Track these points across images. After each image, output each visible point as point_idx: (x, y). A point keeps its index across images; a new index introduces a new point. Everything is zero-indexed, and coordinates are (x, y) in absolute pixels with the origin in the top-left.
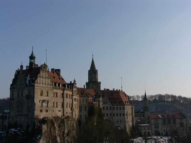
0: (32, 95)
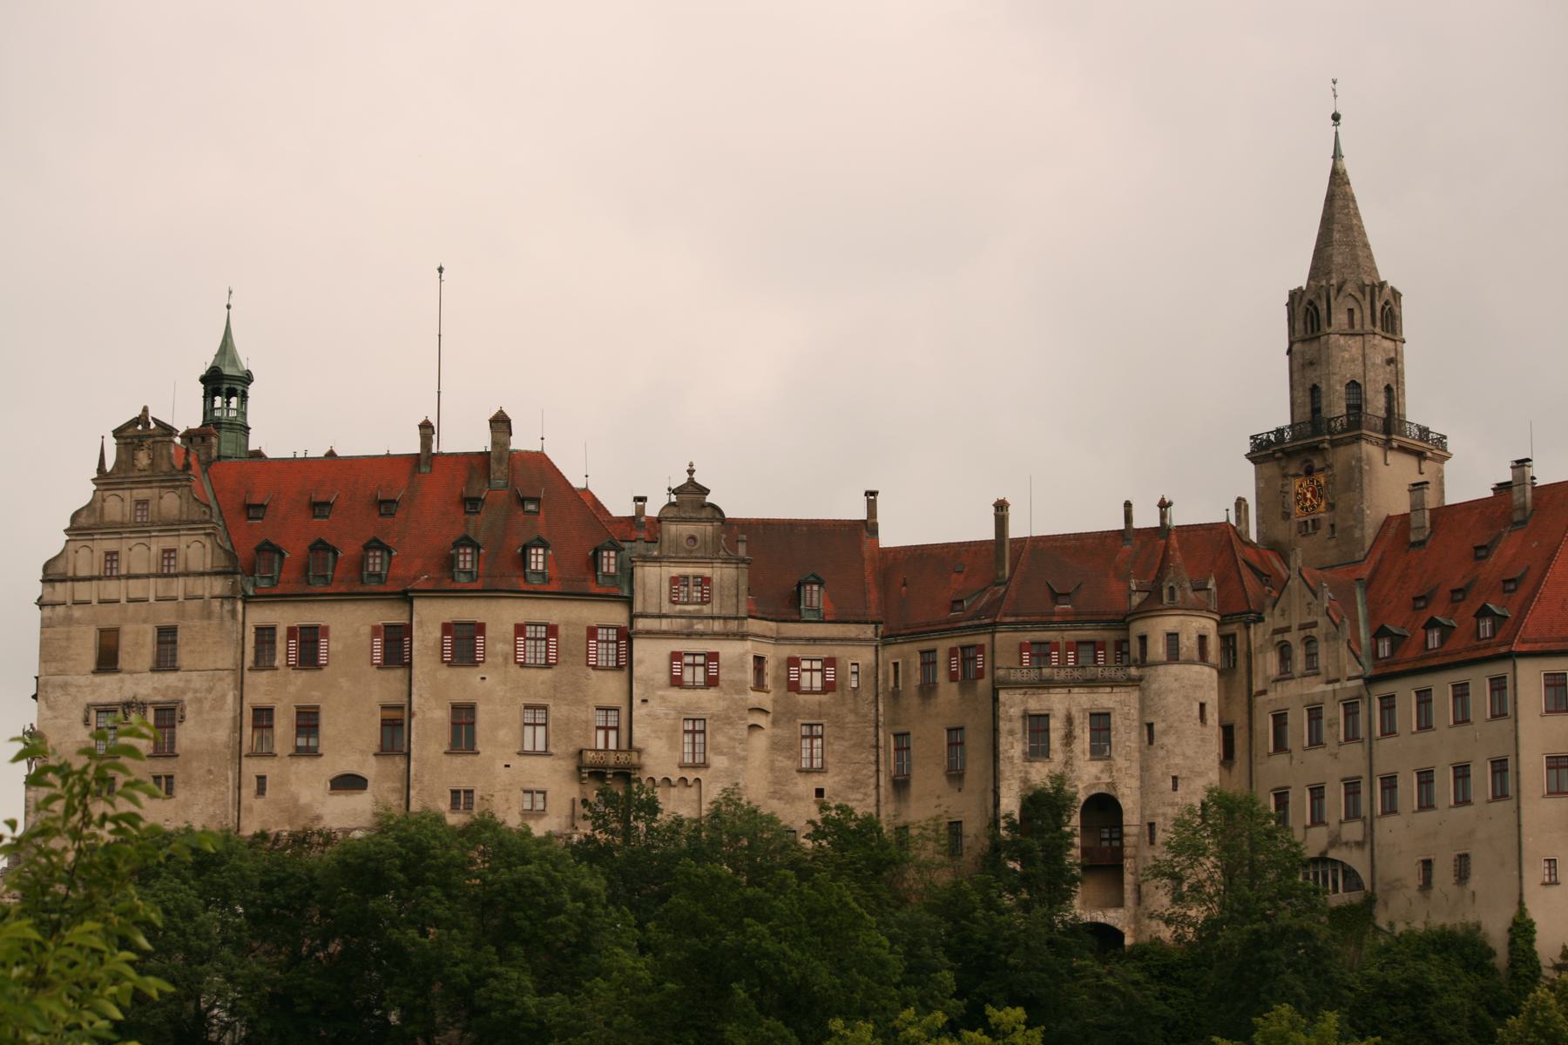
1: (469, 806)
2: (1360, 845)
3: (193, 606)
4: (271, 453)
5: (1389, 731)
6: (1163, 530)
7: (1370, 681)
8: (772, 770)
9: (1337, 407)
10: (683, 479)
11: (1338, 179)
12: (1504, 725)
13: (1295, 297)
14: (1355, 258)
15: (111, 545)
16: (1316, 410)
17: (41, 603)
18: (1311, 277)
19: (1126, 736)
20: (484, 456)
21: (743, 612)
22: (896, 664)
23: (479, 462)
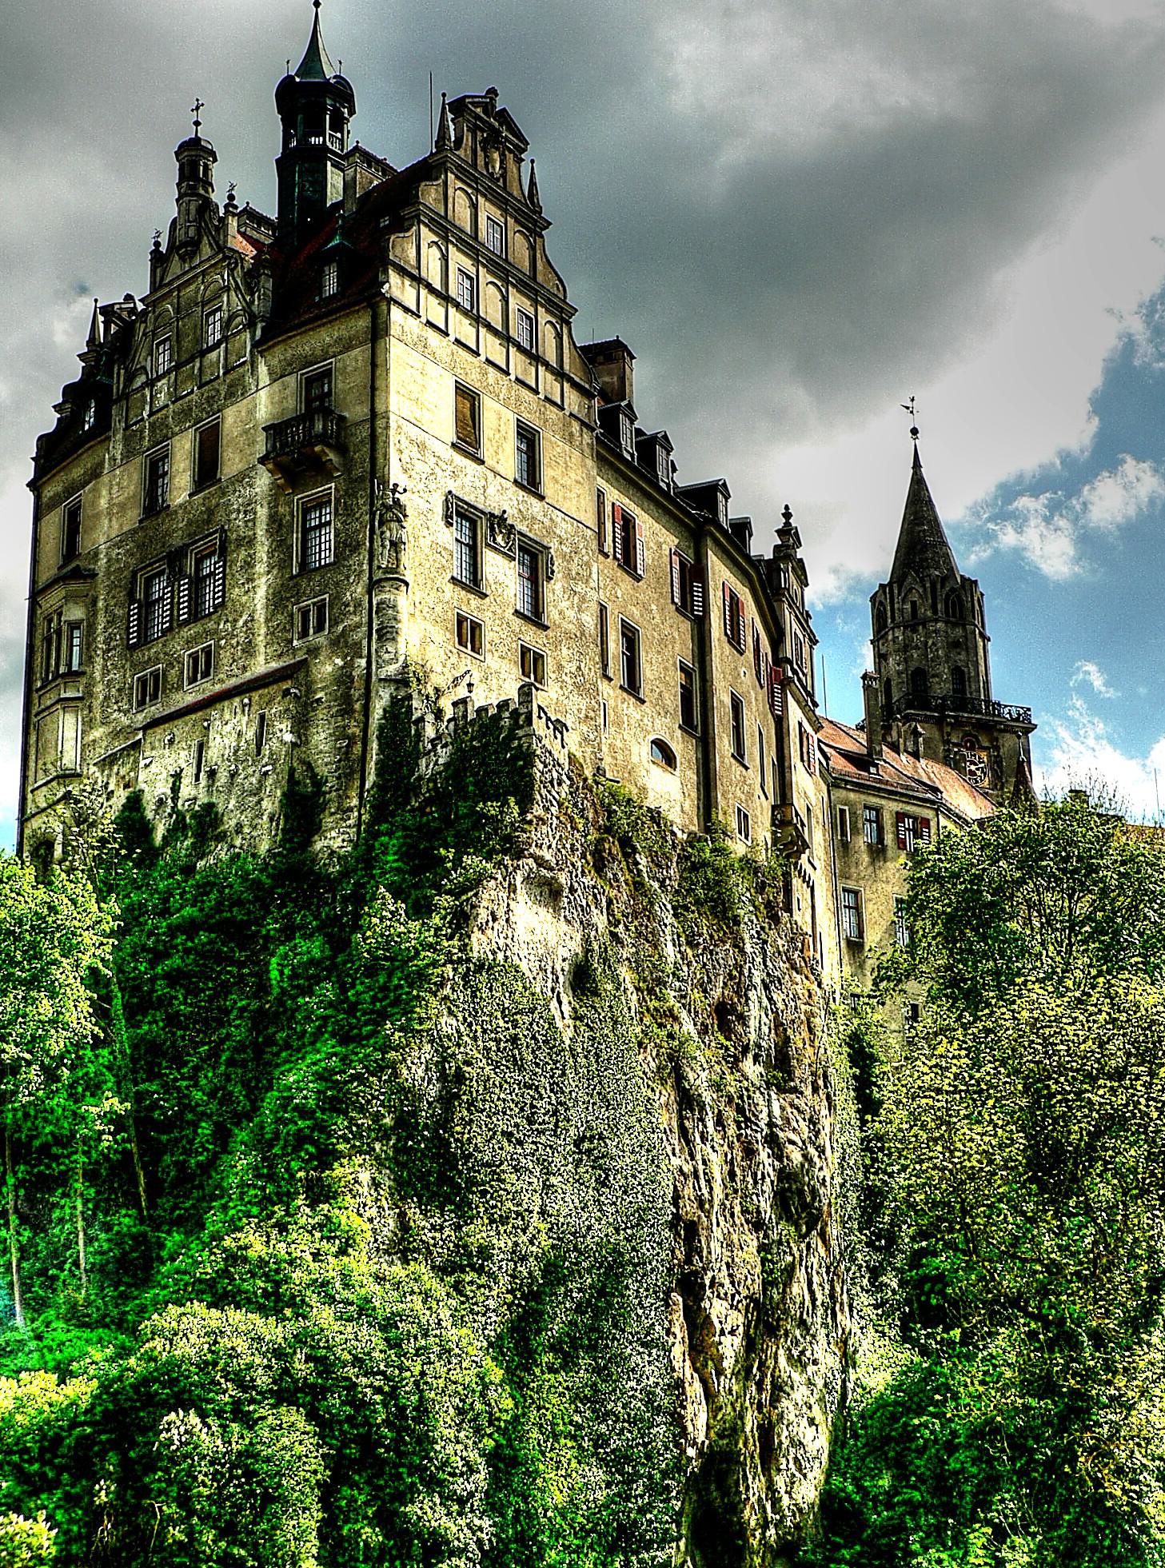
0: (356, 412)
11: (918, 484)
22: (842, 811)
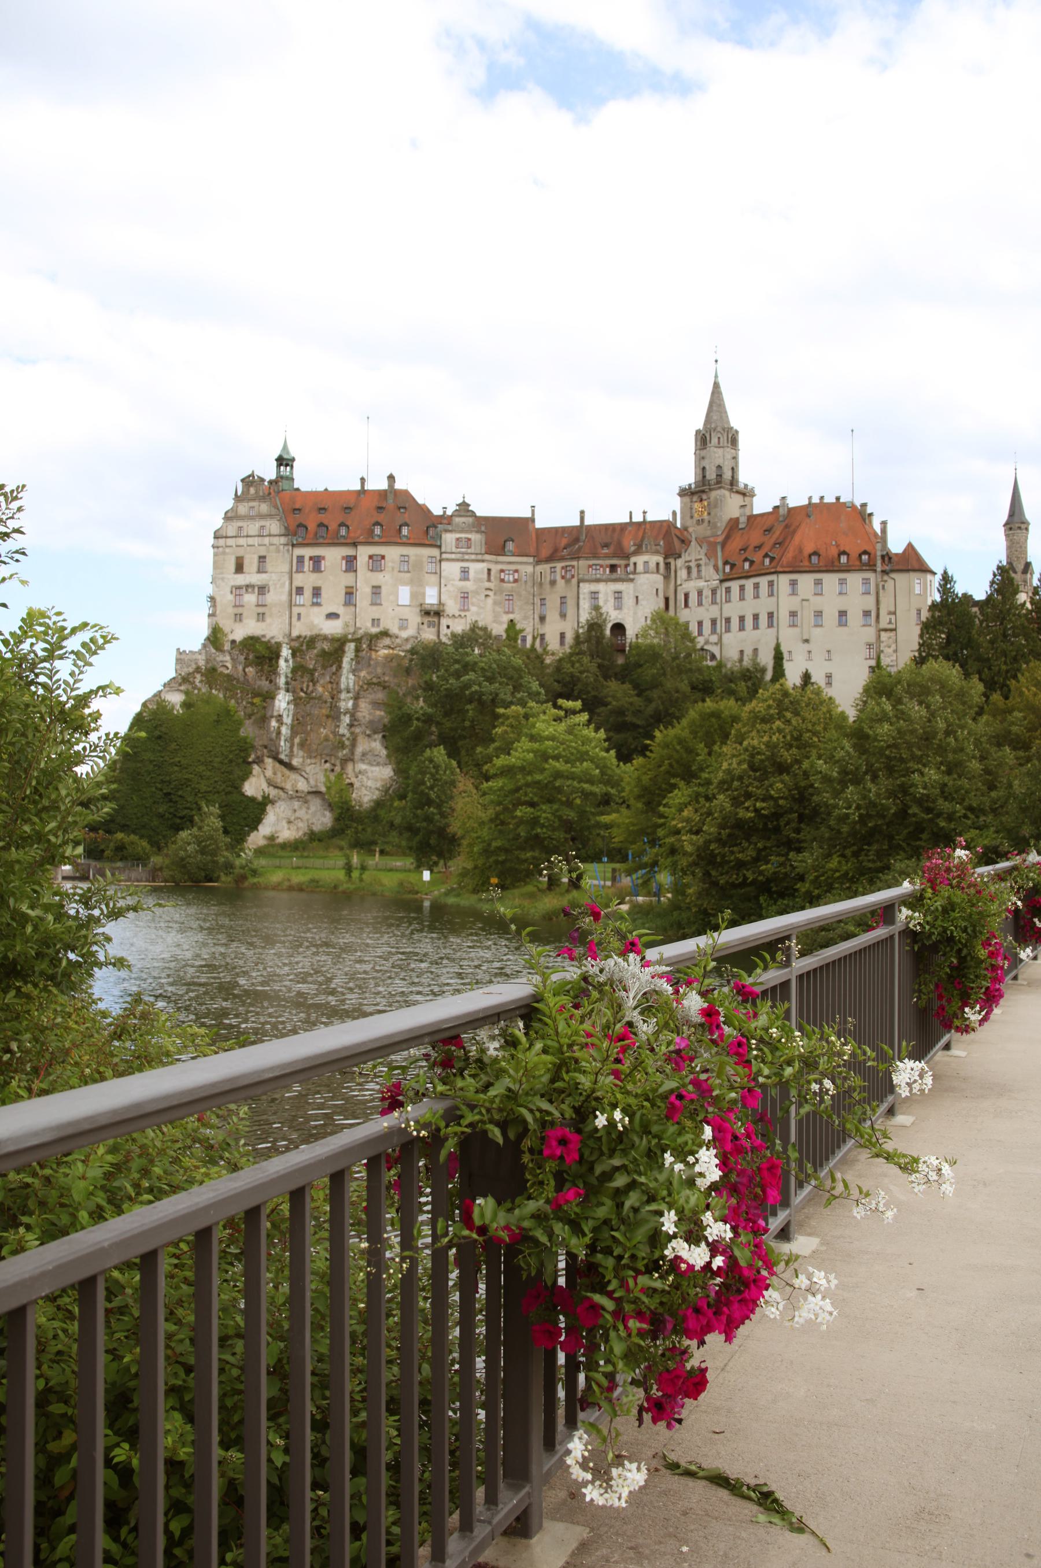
1: (378, 625)
2: (716, 644)
3: (272, 548)
4: (303, 489)
5: (728, 601)
6: (644, 522)
7: (722, 581)
8: (494, 611)
9: (711, 475)
10: (460, 501)
11: (716, 386)
12: (774, 599)
13: (698, 432)
14: (721, 417)
15: (240, 524)
16: (704, 477)
17: (213, 547)
18: (705, 424)
19: (628, 601)
20: (385, 491)
21: (483, 551)
23: (382, 494)
